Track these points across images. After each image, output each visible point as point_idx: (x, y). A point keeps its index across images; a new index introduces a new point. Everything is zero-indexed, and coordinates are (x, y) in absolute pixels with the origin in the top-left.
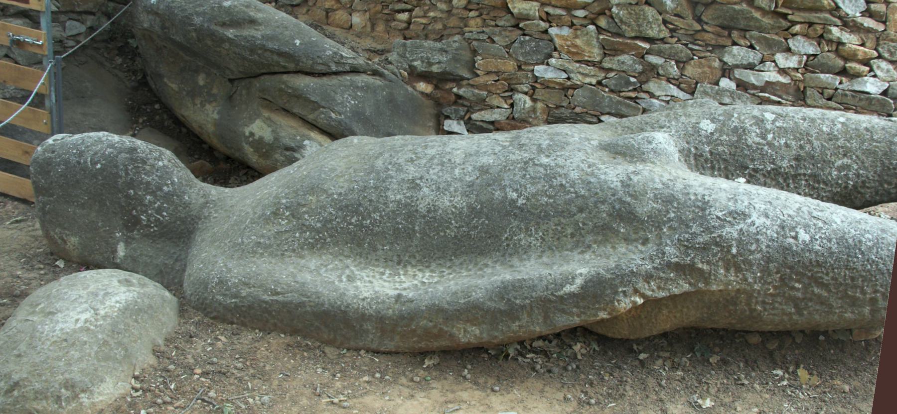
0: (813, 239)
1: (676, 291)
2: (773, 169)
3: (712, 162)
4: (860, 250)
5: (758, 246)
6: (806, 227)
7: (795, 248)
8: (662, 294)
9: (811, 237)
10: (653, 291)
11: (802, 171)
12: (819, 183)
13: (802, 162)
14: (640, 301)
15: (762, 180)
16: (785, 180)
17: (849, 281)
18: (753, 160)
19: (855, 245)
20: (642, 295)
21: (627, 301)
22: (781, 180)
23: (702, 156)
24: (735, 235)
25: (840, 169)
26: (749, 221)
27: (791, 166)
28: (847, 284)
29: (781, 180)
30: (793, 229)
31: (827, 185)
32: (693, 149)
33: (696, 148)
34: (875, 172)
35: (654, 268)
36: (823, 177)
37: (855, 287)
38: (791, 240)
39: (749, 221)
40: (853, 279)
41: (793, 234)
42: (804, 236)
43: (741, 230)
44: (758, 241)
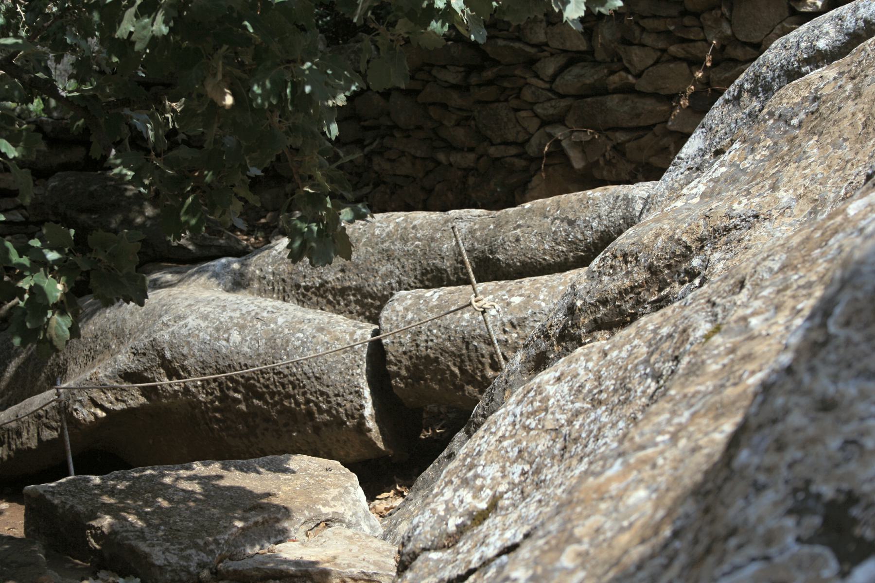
0: (244, 340)
1: (132, 403)
2: (322, 285)
3: (273, 285)
4: (285, 350)
5: (190, 349)
6: (242, 328)
7: (224, 350)
8: (119, 406)
9: (243, 339)
10: (111, 403)
11: (347, 284)
12: (365, 296)
13: (347, 273)
14: (101, 414)
15: (315, 299)
16: (334, 296)
17: (280, 389)
18: (305, 277)
19: (282, 345)
20: (102, 408)
21: (85, 412)
22: (330, 297)
23: (264, 278)
24: (167, 337)
25: (385, 277)
26: (182, 323)
27: (338, 279)
28: (279, 393)
29: (330, 297)
30: (227, 330)
31: (373, 298)
32: (258, 272)
33: (261, 270)
34: (416, 278)
35: (106, 376)
36: (369, 289)
37: (288, 396)
38: (224, 343)
39: (182, 323)
40: (283, 385)
41: (226, 336)
42: (236, 337)
43: (173, 332)
44: (188, 343)
